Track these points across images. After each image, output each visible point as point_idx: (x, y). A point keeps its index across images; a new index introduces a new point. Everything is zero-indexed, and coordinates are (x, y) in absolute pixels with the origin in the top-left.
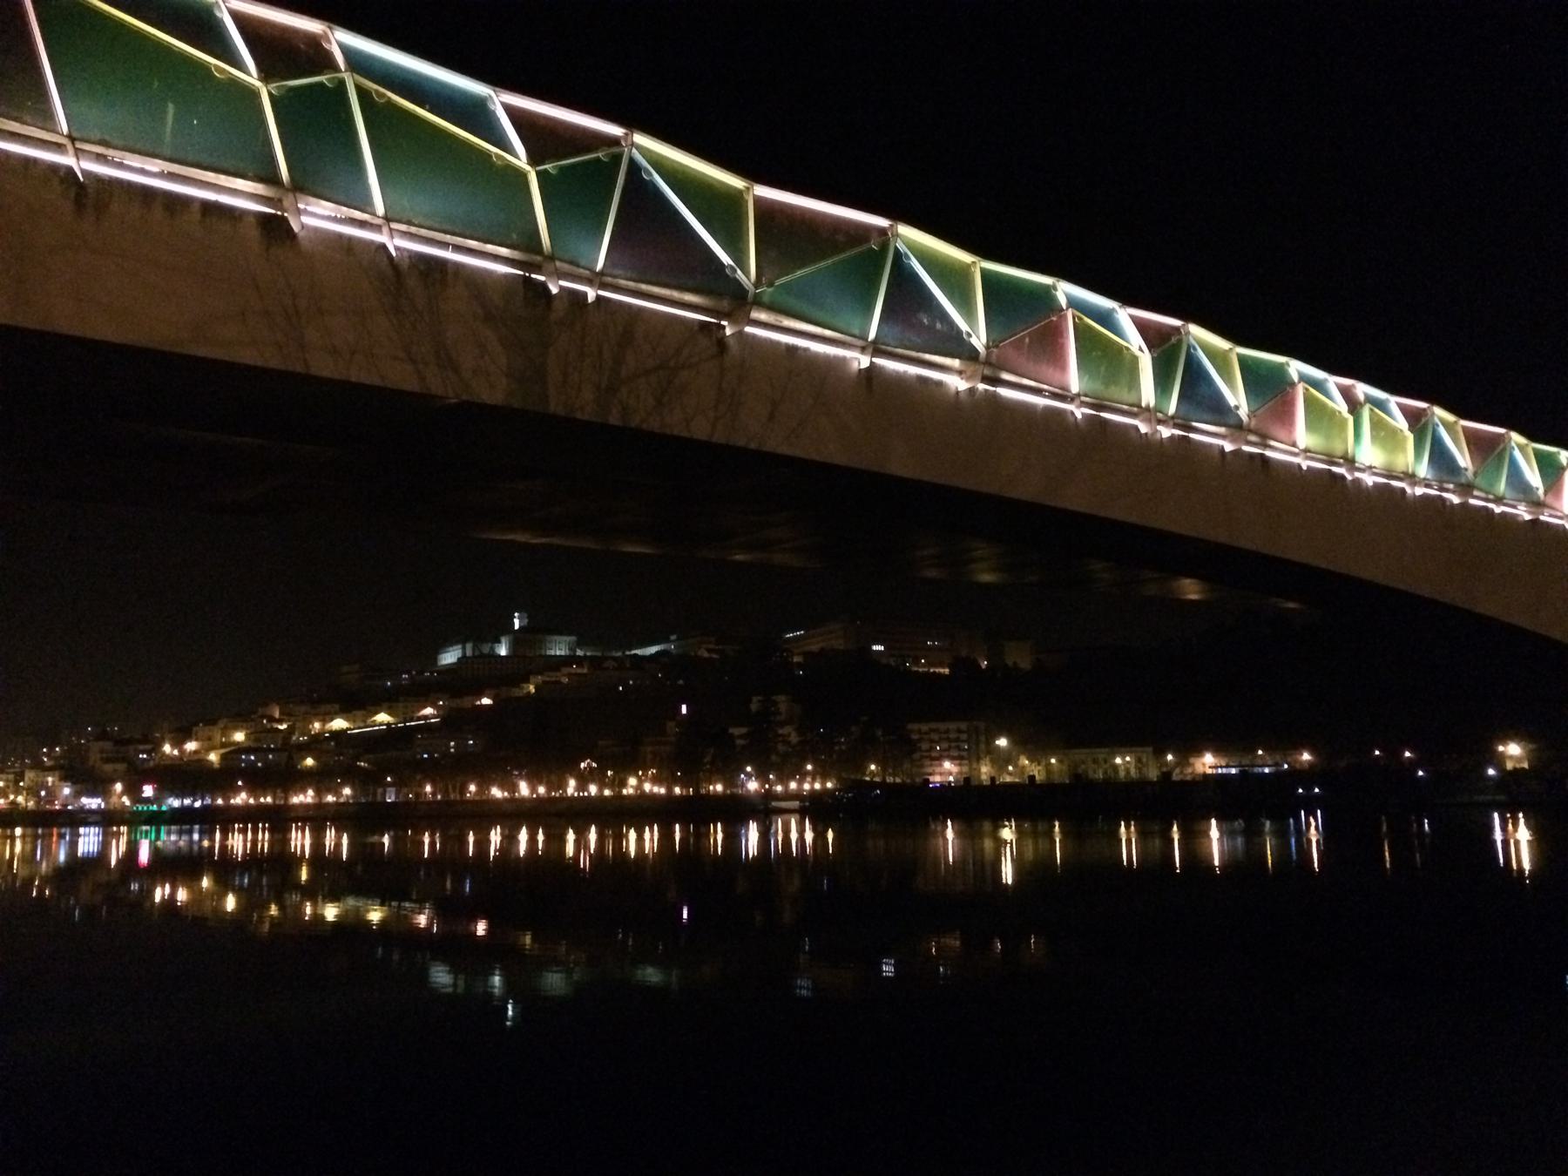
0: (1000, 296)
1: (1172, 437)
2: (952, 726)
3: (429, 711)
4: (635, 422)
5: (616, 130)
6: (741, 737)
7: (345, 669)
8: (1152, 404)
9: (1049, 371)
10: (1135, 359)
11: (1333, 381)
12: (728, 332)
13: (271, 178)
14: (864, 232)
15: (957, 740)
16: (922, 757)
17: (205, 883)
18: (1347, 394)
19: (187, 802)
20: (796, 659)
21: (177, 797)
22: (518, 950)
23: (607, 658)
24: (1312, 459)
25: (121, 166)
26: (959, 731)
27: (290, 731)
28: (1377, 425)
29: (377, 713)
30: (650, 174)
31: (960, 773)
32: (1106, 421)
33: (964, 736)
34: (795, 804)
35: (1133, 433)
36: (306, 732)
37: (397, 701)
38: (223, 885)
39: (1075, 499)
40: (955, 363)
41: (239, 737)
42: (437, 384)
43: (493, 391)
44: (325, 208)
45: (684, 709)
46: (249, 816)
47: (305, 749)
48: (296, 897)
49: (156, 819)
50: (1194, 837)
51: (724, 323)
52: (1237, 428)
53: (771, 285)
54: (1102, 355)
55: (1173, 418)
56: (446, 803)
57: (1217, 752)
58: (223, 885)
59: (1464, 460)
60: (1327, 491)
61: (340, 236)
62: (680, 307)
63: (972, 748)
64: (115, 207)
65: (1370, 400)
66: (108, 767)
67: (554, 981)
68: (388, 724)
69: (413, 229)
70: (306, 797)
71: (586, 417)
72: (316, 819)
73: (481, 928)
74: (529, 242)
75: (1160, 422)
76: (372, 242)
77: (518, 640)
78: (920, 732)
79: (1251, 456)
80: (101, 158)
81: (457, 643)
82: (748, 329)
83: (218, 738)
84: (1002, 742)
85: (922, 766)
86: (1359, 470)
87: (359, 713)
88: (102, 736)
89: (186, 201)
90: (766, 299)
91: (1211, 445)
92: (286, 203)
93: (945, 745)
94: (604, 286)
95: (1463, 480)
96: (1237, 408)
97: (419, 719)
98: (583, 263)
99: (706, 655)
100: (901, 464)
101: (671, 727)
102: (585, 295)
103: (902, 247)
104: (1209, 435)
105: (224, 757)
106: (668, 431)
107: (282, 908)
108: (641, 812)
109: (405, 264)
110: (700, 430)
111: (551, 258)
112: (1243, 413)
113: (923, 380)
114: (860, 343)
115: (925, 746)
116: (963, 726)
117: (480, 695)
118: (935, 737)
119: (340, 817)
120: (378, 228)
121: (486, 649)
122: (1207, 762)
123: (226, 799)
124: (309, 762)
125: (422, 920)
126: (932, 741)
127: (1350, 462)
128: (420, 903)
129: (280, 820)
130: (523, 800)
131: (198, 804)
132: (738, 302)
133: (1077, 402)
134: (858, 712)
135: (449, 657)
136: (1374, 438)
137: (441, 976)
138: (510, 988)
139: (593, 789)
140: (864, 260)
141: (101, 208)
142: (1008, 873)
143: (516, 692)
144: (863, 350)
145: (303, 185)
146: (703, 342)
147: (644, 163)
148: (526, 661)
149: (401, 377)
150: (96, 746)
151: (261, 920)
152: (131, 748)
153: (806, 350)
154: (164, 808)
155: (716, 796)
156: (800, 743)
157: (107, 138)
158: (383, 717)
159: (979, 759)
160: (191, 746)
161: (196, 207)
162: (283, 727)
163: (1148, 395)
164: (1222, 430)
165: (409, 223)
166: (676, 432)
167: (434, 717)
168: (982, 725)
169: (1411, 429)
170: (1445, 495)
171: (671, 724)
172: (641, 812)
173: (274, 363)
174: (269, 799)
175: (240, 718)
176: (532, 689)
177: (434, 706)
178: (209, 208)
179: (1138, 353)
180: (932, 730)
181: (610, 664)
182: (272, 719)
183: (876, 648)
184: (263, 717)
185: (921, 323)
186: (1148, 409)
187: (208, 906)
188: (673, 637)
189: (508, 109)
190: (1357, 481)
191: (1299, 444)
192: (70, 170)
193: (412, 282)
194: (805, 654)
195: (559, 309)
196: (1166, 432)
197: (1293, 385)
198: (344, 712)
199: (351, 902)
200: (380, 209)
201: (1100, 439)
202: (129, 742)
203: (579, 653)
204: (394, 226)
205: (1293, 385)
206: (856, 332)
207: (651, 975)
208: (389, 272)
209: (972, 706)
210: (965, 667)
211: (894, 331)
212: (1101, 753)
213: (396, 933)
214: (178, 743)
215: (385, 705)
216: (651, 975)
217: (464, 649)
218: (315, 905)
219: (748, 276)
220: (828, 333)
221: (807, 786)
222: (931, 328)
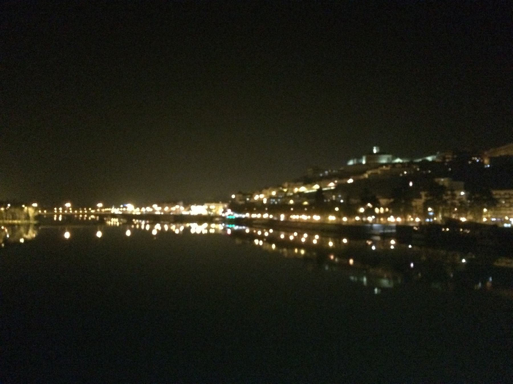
36: (292, 192)
41: (274, 193)
47: (291, 197)
67: (385, 282)
73: (351, 261)
87: (309, 185)
117: (349, 178)
124: (292, 202)
143: (362, 177)
154: (234, 217)
160: (262, 196)
162: (285, 190)
176: (366, 176)
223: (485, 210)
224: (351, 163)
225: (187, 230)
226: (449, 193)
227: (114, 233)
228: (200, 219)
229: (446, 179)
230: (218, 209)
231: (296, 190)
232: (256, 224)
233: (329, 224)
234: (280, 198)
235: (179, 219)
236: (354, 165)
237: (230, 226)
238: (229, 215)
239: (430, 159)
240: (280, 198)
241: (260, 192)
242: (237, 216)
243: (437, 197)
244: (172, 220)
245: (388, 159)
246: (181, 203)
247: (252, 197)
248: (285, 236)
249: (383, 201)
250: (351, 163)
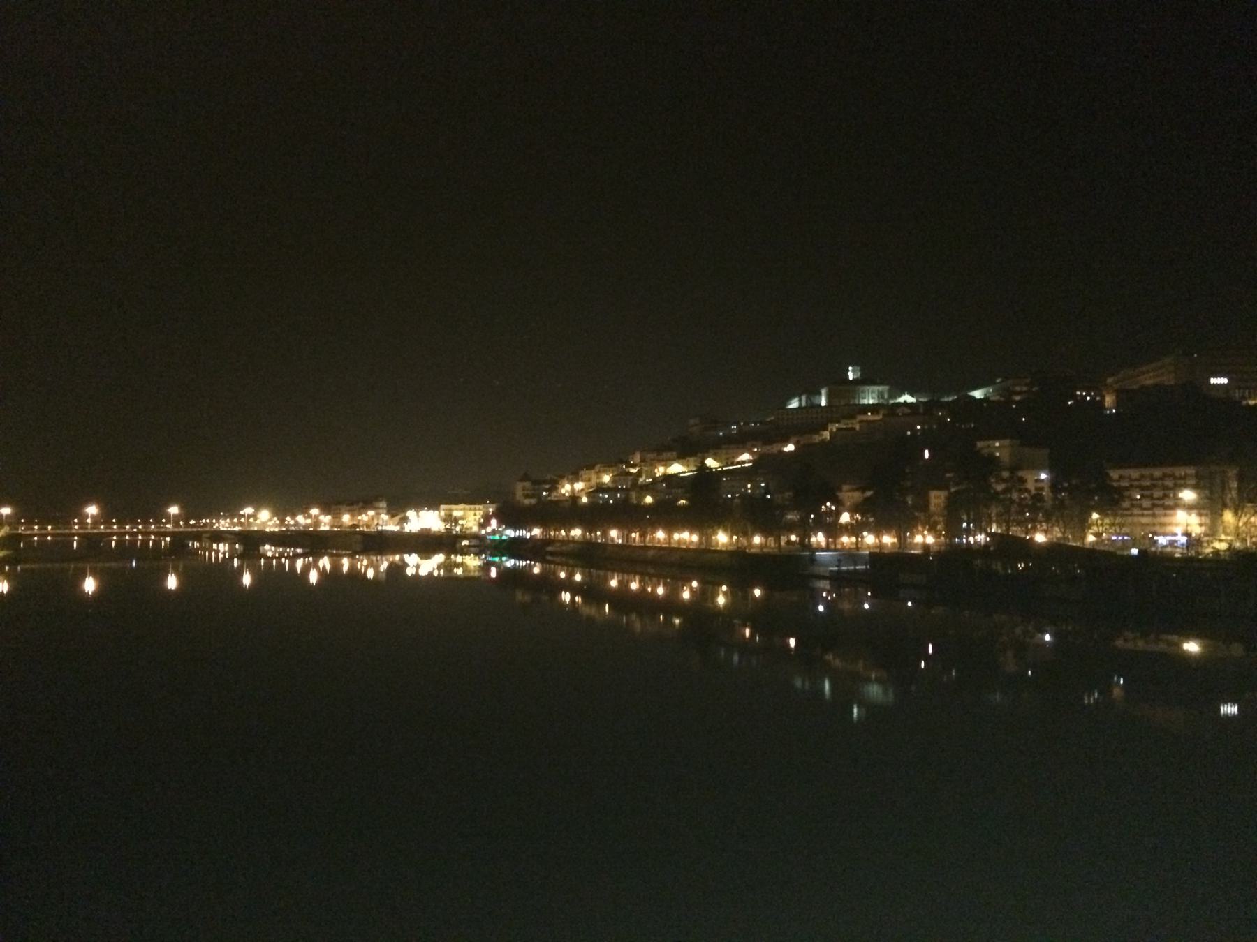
3: (746, 457)
16: (1154, 506)
27: (639, 474)
41: (606, 479)
45: (927, 454)
47: (646, 489)
73: (792, 642)
78: (1152, 478)
117: (786, 441)
123: (568, 532)
124: (649, 500)
126: (1166, 488)
143: (817, 439)
150: (520, 486)
154: (504, 538)
160: (579, 486)
162: (633, 471)
167: (750, 461)
175: (608, 465)
176: (826, 435)
177: (751, 453)
180: (1164, 476)
184: (622, 462)
198: (681, 457)
217: (800, 401)
223: (1095, 516)
224: (794, 404)
225: (397, 570)
226: (1006, 474)
227: (210, 582)
228: (426, 544)
229: (1007, 442)
230: (470, 518)
231: (660, 471)
232: (552, 554)
233: (721, 552)
235: (378, 543)
236: (800, 408)
237: (497, 559)
238: (494, 532)
239: (978, 394)
241: (575, 477)
242: (510, 533)
243: (975, 487)
244: (358, 547)
245: (881, 395)
246: (383, 504)
247: (554, 486)
248: (619, 582)
249: (850, 495)
250: (794, 404)
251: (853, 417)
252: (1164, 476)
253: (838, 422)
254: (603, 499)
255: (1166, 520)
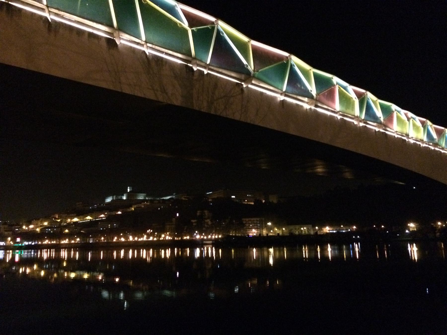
0: (319, 80)
1: (363, 126)
2: (255, 219)
3: (102, 216)
4: (218, 113)
5: (212, 19)
6: (194, 223)
7: (77, 203)
8: (359, 115)
9: (330, 103)
10: (354, 101)
11: (403, 111)
12: (244, 86)
13: (110, 25)
14: (280, 58)
15: (257, 223)
16: (247, 228)
17: (35, 267)
18: (406, 115)
19: (30, 243)
20: (210, 200)
21: (27, 241)
22: (129, 286)
23: (154, 200)
24: (398, 134)
25: (62, 17)
26: (257, 221)
27: (61, 222)
28: (414, 125)
29: (87, 216)
30: (223, 34)
31: (257, 233)
32: (345, 120)
33: (258, 222)
34: (211, 242)
35: (353, 124)
37: (93, 213)
38: (41, 268)
39: (339, 143)
40: (306, 99)
41: (46, 224)
42: (161, 98)
43: (177, 101)
44: (126, 36)
45: (178, 215)
46: (49, 247)
48: (62, 271)
49: (20, 248)
50: (324, 250)
51: (243, 83)
52: (380, 124)
53: (258, 71)
54: (345, 99)
55: (363, 120)
56: (107, 243)
57: (330, 226)
58: (41, 268)
59: (435, 136)
60: (401, 145)
61: (131, 47)
62: (229, 77)
63: (262, 225)
64: (61, 31)
65: (412, 117)
66: (6, 233)
67: (139, 295)
68: (90, 220)
69: (154, 46)
70: (66, 241)
71: (204, 111)
72: (68, 247)
73: (117, 280)
74: (188, 53)
75: (361, 121)
76: (140, 50)
77: (129, 195)
78: (246, 221)
79: (383, 133)
80: (57, 15)
81: (110, 196)
82: (250, 86)
83: (39, 224)
84: (269, 224)
85: (246, 231)
86: (410, 138)
88: (5, 224)
89: (83, 32)
90: (256, 76)
91: (372, 129)
92: (115, 35)
93: (253, 225)
94: (210, 69)
95: (435, 142)
96: (380, 118)
97: (100, 218)
98: (203, 61)
99: (184, 199)
100: (292, 131)
101: (174, 219)
102: (203, 72)
103: (293, 63)
104: (373, 126)
105: (41, 230)
106: (228, 117)
107: (58, 274)
108: (165, 245)
109: (151, 58)
110: (237, 117)
111: (195, 58)
112: (382, 119)
113: (297, 105)
114: (280, 91)
115: (247, 225)
116: (258, 219)
117: (118, 211)
118: (250, 222)
119: (76, 247)
120: (142, 45)
121: (119, 197)
122: (327, 229)
124: (67, 231)
125: (100, 278)
127: (407, 135)
128: (100, 272)
129: (58, 248)
130: (130, 242)
131: (33, 244)
132: (248, 76)
133: (338, 114)
134: (228, 216)
135: (109, 200)
136: (413, 128)
137: (105, 294)
138: (126, 298)
139: (151, 238)
140: (282, 66)
141: (56, 32)
142: (271, 261)
143: (129, 210)
144: (281, 94)
145: (121, 29)
146: (237, 89)
147: (222, 30)
148: (131, 201)
149: (150, 95)
151: (52, 278)
152: (13, 227)
153: (265, 93)
154: (23, 245)
155: (187, 240)
156: (211, 224)
157: (59, 8)
158: (89, 218)
159: (262, 229)
160: (31, 226)
161: (86, 35)
163: (357, 112)
164: (375, 124)
165: (152, 44)
166: (230, 117)
167: (104, 217)
168: (263, 219)
169: (422, 126)
170: (430, 147)
171: (174, 219)
172: (165, 245)
173: (111, 88)
174: (55, 242)
175: (46, 218)
176: (133, 209)
178: (90, 34)
179: (354, 99)
180: (249, 221)
181: (156, 202)
182: (55, 218)
183: (233, 197)
184: (53, 218)
185: (298, 86)
186: (357, 117)
187: (36, 274)
188: (174, 194)
189: (182, 10)
190: (408, 141)
191: (394, 130)
192: (46, 18)
193: (153, 64)
194: (213, 199)
195: (196, 76)
196: (362, 124)
197: (393, 112)
198: (77, 216)
199: (78, 273)
200: (144, 38)
201: (344, 125)
202: (13, 225)
203: (147, 198)
204: (148, 45)
205: (393, 112)
206: (280, 88)
207: (167, 293)
208: (146, 60)
209: (261, 213)
210: (258, 202)
211: (290, 89)
212: (297, 227)
213: (92, 281)
214: (27, 226)
215: (90, 214)
216: (167, 293)
217: (113, 198)
218: (68, 273)
219: (251, 67)
220: (271, 88)
221: (213, 237)
222: (300, 88)
231: (69, 220)
234: (55, 228)
240: (55, 228)
241: (29, 223)
242: (26, 243)
251: (141, 203)
252: (249, 221)
253: (135, 204)
254: (48, 231)
255: (249, 232)
